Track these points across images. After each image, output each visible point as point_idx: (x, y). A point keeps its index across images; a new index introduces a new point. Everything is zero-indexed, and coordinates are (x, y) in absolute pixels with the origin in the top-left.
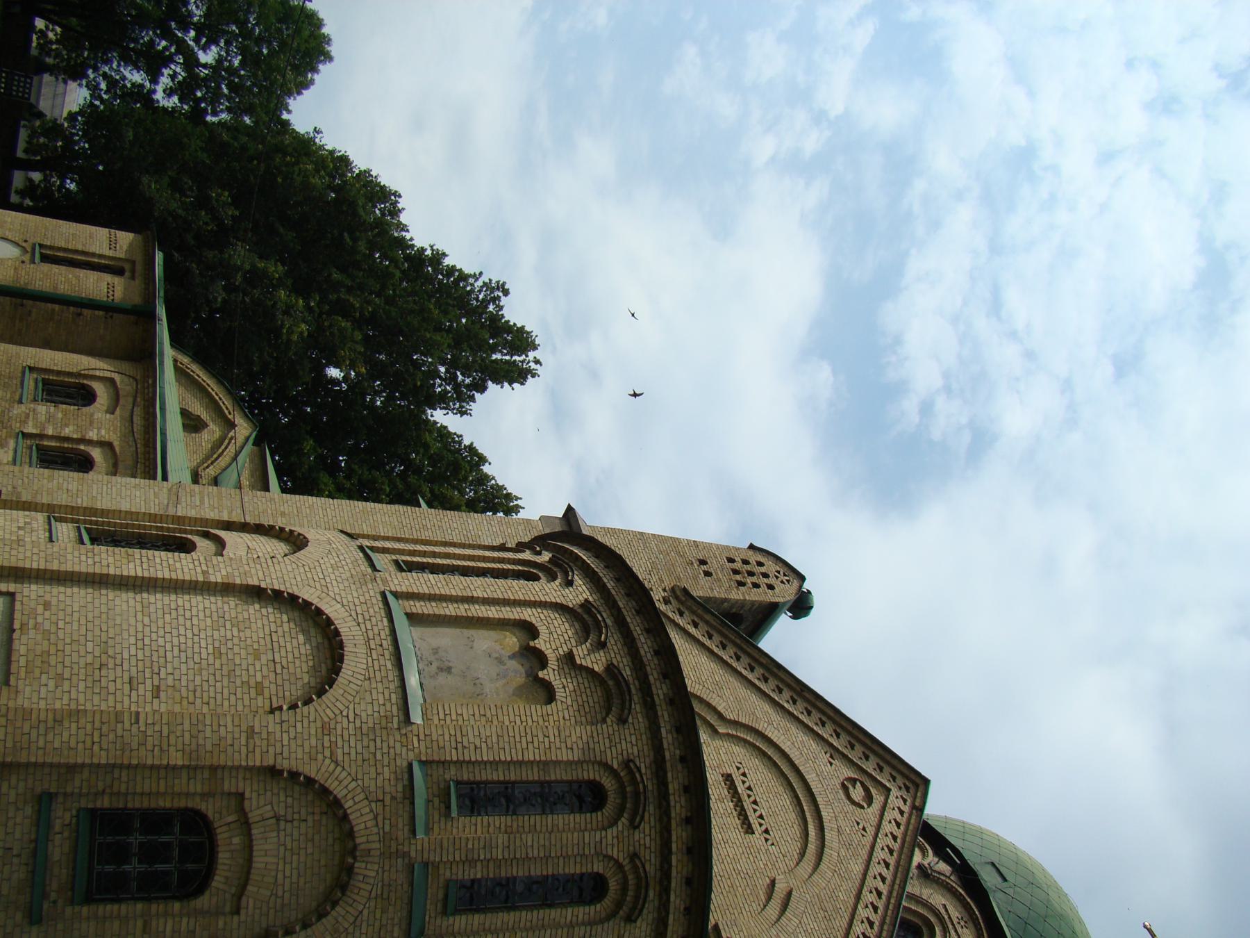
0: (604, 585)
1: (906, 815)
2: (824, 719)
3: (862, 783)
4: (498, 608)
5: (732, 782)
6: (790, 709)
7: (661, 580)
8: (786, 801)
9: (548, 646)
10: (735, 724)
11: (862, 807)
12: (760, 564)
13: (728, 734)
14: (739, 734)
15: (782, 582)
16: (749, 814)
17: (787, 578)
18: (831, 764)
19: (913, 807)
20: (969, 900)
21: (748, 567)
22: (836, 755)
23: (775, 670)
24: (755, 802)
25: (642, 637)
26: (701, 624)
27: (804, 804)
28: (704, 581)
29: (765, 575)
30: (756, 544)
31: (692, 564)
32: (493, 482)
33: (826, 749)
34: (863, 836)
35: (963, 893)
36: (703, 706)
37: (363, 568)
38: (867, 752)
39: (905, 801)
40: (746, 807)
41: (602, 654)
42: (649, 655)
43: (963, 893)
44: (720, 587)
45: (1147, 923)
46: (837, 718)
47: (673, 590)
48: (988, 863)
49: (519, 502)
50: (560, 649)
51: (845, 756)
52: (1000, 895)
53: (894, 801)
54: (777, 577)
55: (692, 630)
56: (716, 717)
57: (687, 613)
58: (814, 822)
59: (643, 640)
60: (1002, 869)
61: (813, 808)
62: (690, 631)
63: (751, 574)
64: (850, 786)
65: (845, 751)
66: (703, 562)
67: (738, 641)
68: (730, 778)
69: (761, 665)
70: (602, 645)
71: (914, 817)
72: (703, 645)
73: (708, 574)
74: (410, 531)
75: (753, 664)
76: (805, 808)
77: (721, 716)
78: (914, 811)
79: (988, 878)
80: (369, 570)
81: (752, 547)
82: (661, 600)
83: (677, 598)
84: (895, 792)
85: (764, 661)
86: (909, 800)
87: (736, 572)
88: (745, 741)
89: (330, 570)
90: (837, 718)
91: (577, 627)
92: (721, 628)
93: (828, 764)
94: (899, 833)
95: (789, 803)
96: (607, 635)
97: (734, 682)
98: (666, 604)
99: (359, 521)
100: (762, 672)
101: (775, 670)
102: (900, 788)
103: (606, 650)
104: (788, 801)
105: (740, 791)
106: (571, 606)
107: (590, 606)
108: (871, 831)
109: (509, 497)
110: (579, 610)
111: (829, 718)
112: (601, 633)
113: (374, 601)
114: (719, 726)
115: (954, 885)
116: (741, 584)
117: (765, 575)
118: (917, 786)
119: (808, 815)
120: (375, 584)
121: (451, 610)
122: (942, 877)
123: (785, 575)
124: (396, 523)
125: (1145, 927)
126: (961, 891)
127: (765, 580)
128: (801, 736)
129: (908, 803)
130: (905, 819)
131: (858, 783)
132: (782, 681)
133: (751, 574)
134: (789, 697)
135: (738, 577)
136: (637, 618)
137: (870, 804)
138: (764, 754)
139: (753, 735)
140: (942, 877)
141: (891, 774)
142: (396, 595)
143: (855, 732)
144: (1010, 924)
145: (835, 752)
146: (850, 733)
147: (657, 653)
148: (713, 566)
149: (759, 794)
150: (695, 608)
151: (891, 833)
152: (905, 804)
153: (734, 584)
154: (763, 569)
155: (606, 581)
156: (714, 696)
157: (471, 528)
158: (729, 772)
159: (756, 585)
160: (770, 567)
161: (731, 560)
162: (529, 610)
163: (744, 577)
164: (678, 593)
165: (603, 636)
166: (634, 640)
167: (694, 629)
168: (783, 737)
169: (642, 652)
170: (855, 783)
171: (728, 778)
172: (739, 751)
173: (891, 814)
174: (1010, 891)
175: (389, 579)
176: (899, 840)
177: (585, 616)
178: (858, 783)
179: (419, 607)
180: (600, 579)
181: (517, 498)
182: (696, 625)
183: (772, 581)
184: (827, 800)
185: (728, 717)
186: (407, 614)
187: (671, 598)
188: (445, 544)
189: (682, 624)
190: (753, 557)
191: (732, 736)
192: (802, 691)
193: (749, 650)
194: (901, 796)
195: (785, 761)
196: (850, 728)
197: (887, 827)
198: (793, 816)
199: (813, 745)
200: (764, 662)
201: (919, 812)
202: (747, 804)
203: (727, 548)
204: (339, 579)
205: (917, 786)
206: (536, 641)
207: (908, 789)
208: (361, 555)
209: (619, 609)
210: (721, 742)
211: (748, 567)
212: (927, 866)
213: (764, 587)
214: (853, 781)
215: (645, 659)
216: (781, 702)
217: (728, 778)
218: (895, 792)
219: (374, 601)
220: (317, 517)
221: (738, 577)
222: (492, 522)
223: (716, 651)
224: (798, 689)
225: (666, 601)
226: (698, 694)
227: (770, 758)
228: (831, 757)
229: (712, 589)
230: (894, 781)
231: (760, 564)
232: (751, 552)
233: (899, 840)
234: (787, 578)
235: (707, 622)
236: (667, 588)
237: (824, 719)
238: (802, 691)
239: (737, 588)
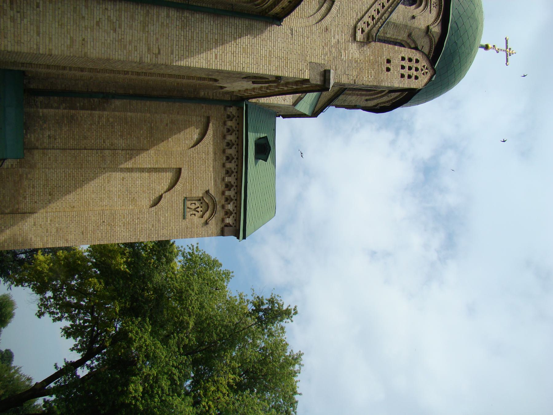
45: (507, 38)
125: (506, 39)
144: (454, 14)
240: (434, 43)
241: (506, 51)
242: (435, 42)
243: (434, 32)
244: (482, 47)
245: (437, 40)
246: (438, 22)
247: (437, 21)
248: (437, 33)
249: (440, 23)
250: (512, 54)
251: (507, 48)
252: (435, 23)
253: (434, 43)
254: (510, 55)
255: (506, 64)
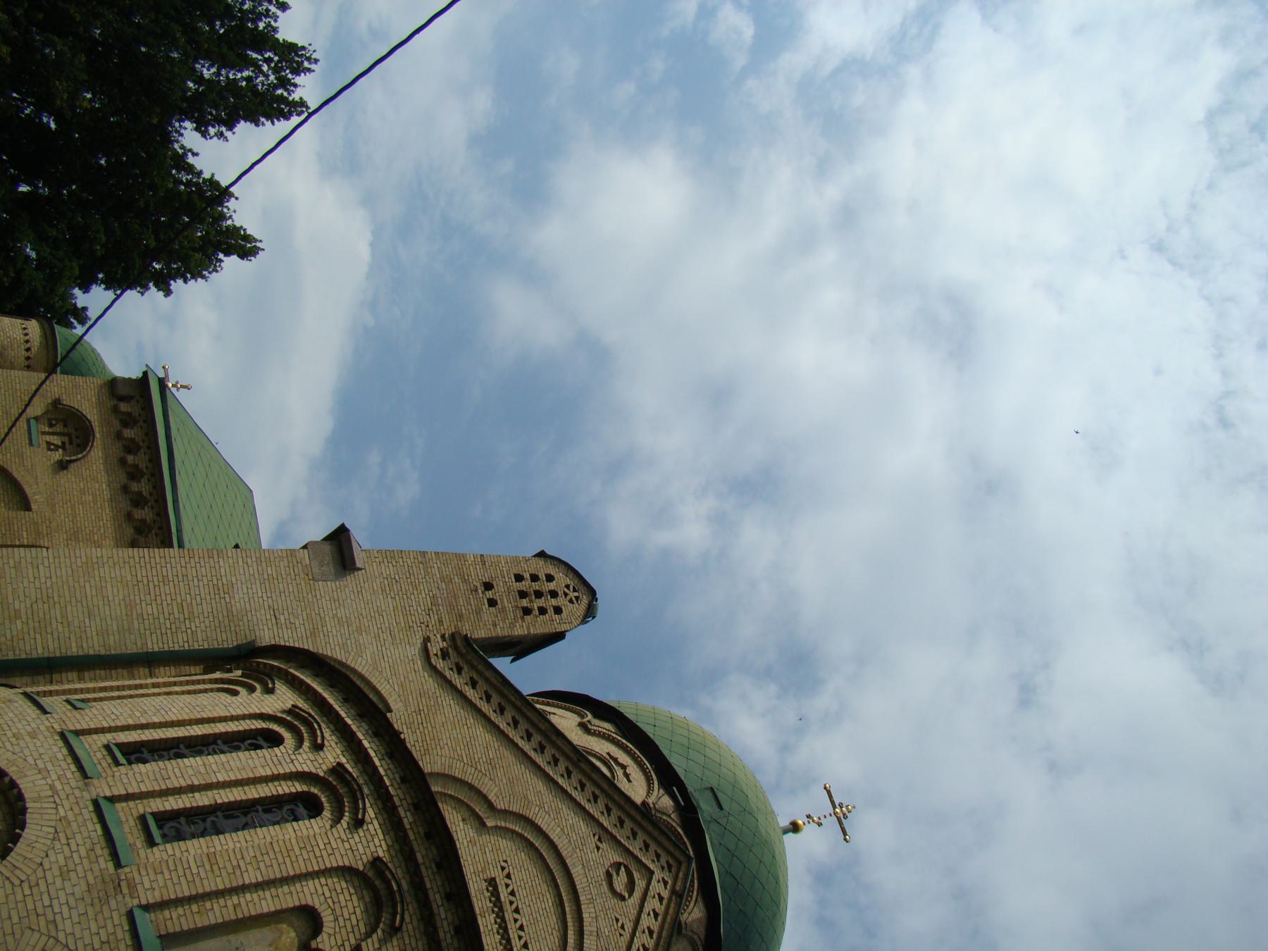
0: (400, 821)
1: (665, 902)
2: (597, 792)
3: (626, 867)
4: (273, 890)
5: (496, 888)
6: (564, 786)
7: (441, 621)
8: (549, 901)
9: (333, 943)
10: (506, 813)
11: (623, 898)
12: (550, 578)
13: (496, 827)
14: (507, 825)
15: (571, 601)
16: (509, 927)
17: (576, 594)
18: (598, 848)
19: (673, 892)
20: (686, 840)
21: (536, 586)
22: (604, 836)
23: (554, 738)
24: (517, 911)
25: (441, 909)
26: (480, 682)
27: (566, 905)
28: (488, 613)
29: (554, 594)
30: (548, 552)
31: (476, 590)
32: (229, 222)
33: (597, 830)
34: (621, 935)
35: (681, 832)
36: (472, 795)
37: (103, 865)
38: (636, 829)
39: (665, 883)
40: (507, 919)
41: (395, 943)
42: (448, 936)
43: (681, 832)
44: (504, 620)
45: (827, 785)
46: (611, 792)
47: (453, 636)
48: (706, 789)
49: (258, 244)
50: (347, 944)
51: (613, 837)
52: (714, 826)
53: (656, 887)
54: (566, 595)
55: (469, 692)
56: (485, 806)
57: (466, 668)
58: (574, 926)
59: (443, 916)
60: (720, 795)
61: (574, 908)
62: (468, 694)
63: (539, 594)
64: (614, 874)
65: (614, 831)
66: (488, 586)
67: (518, 703)
68: (493, 883)
69: (539, 730)
70: (394, 930)
71: (672, 905)
72: (479, 711)
73: (492, 603)
74: (146, 588)
75: (531, 730)
76: (567, 909)
77: (491, 806)
78: (674, 898)
79: (706, 808)
80: (111, 865)
81: (542, 555)
82: (439, 653)
83: (456, 648)
84: (658, 874)
85: (542, 726)
86: (670, 882)
87: (523, 594)
88: (513, 832)
89: (59, 881)
90: (611, 792)
91: (367, 899)
92: (502, 687)
93: (596, 850)
94: (655, 926)
95: (551, 904)
96: (402, 919)
97: (508, 756)
98: (444, 659)
99: (81, 580)
100: (540, 739)
101: (554, 738)
102: (663, 868)
103: (399, 935)
104: (550, 900)
105: (503, 899)
106: (361, 868)
107: (384, 868)
108: (629, 926)
109: (248, 238)
110: (370, 874)
111: (603, 790)
112: (394, 914)
113: (120, 936)
114: (488, 818)
115: (674, 824)
116: (527, 611)
117: (554, 594)
118: (680, 863)
119: (569, 917)
120: (120, 897)
121: (218, 912)
122: (665, 817)
123: (575, 590)
124: (129, 579)
125: (825, 788)
126: (679, 830)
127: (554, 602)
128: (571, 818)
129: (668, 887)
130: (663, 908)
131: (623, 869)
132: (558, 748)
133: (539, 594)
134: (564, 769)
135: (525, 603)
136: (438, 878)
137: (631, 892)
138: (531, 845)
139: (522, 823)
140: (665, 817)
141: (656, 851)
142: (147, 908)
143: (627, 807)
144: (719, 858)
145: (604, 834)
146: (621, 808)
147: (457, 930)
148: (499, 592)
149: (522, 900)
150: (475, 663)
151: (649, 928)
152: (666, 888)
153: (519, 613)
154: (552, 586)
155: (402, 814)
156: (487, 779)
157: (223, 574)
158: (493, 876)
159: (543, 611)
160: (561, 580)
161: (519, 578)
162: (311, 882)
163: (531, 601)
164: (459, 643)
165: (398, 918)
166: (432, 914)
167: (471, 690)
168: (553, 823)
169: (441, 934)
170: (619, 869)
171: (492, 882)
172: (506, 846)
173: (651, 904)
174: (723, 821)
175: (137, 881)
176: (655, 936)
177: (377, 882)
178: (623, 869)
179: (179, 920)
180: (394, 808)
181: (256, 241)
182: (474, 684)
183: (560, 601)
184: (590, 896)
185: (499, 808)
186: (160, 937)
187: (450, 650)
188: (195, 692)
189: (459, 686)
190: (543, 568)
191: (500, 828)
192: (579, 760)
193: (529, 714)
194: (663, 878)
195: (551, 851)
196: (622, 803)
197: (647, 921)
198: (553, 920)
199: (583, 828)
200: (543, 728)
201: (678, 899)
202: (509, 916)
203: (516, 560)
204: (72, 902)
205: (680, 863)
206: (319, 939)
207: (670, 866)
208: (98, 827)
209: (417, 865)
210: (487, 836)
211: (536, 586)
212: (652, 806)
213: (551, 611)
214: (617, 866)
215: (444, 944)
216: (555, 777)
217: (492, 882)
218: (658, 874)
219: (120, 936)
220: (26, 581)
221: (525, 603)
222: (249, 561)
223: (493, 719)
224: (575, 759)
225: (444, 655)
226: (469, 781)
227: (536, 849)
228: (599, 840)
229: (495, 625)
230: (658, 861)
231: (550, 578)
232: (541, 562)
233: (655, 936)
234: (576, 594)
235: (487, 680)
236: (447, 635)
237: (597, 792)
238: (579, 760)
239: (522, 618)
240: (699, 943)
241: (835, 813)
242: (700, 939)
243: (693, 921)
244: (785, 831)
245: (702, 931)
246: (694, 898)
247: (691, 897)
248: (699, 920)
249: (699, 898)
250: (849, 812)
251: (834, 807)
252: (690, 902)
253: (699, 943)
254: (845, 817)
255: (845, 839)
